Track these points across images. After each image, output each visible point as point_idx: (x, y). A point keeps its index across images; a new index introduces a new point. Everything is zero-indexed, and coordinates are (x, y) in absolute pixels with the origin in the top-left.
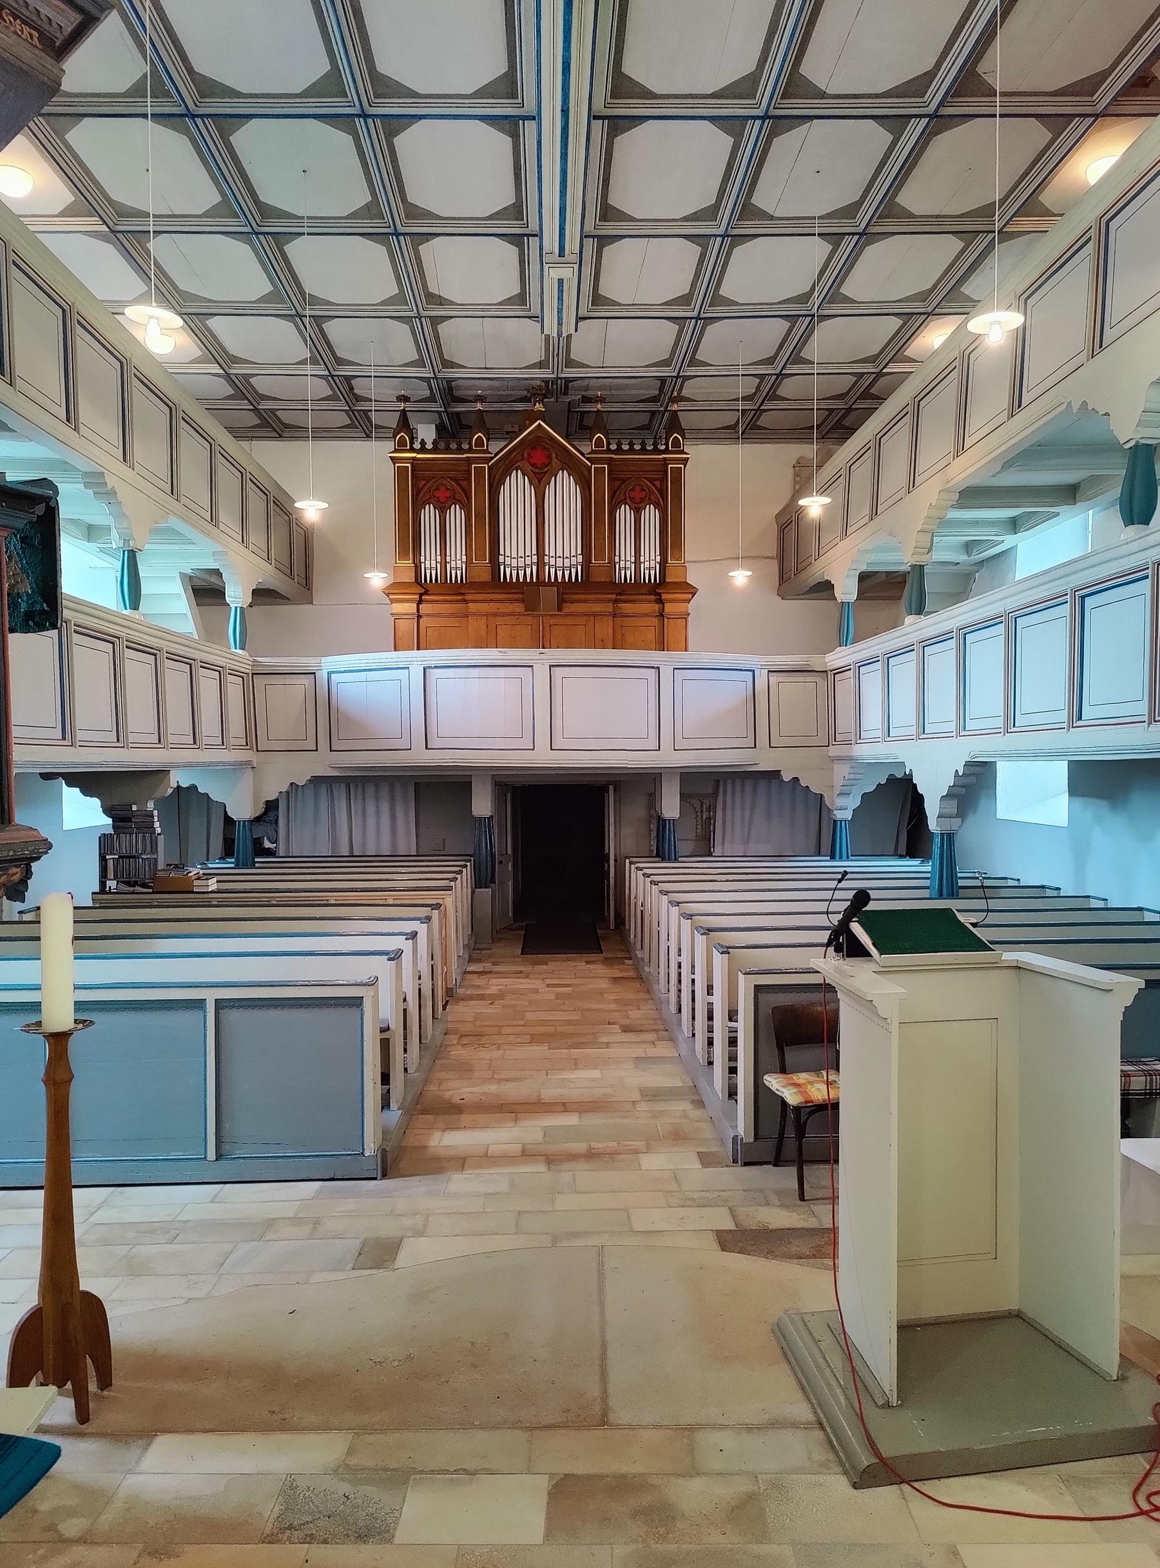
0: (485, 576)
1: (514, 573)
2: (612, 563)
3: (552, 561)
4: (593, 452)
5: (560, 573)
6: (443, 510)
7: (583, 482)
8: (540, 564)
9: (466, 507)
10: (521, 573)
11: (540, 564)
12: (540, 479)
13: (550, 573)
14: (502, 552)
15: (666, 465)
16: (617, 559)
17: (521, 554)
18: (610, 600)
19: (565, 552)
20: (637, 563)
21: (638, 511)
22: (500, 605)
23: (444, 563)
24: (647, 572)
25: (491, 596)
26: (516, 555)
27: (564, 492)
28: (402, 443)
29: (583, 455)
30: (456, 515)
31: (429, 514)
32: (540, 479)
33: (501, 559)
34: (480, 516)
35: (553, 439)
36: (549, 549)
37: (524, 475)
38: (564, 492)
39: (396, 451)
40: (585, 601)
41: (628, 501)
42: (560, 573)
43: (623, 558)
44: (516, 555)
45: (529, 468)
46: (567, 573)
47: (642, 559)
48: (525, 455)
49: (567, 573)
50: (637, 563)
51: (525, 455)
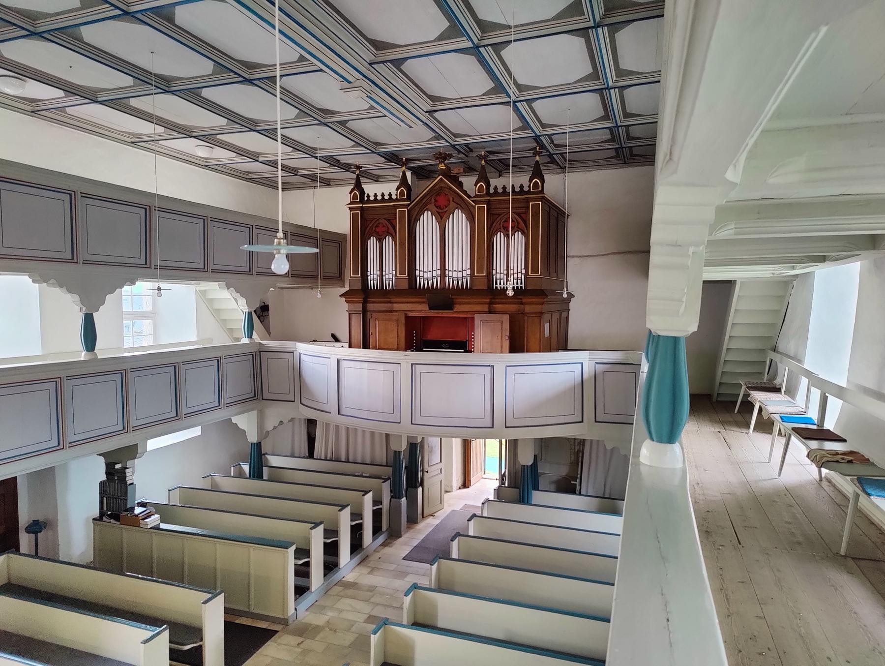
0: (405, 286)
1: (426, 282)
2: (490, 276)
3: (451, 274)
4: (476, 196)
6: (380, 241)
7: (471, 218)
8: (443, 275)
10: (430, 282)
11: (443, 275)
12: (442, 217)
13: (449, 282)
14: (418, 268)
15: (528, 203)
16: (494, 272)
18: (485, 303)
19: (459, 267)
22: (414, 305)
23: (382, 276)
25: (406, 300)
26: (427, 270)
27: (459, 224)
28: (355, 197)
29: (469, 197)
30: (388, 243)
31: (372, 243)
32: (442, 217)
34: (402, 244)
35: (450, 188)
36: (449, 265)
37: (433, 214)
38: (459, 224)
40: (469, 303)
41: (502, 230)
42: (455, 282)
44: (427, 270)
45: (435, 209)
46: (455, 282)
47: (511, 272)
49: (460, 282)
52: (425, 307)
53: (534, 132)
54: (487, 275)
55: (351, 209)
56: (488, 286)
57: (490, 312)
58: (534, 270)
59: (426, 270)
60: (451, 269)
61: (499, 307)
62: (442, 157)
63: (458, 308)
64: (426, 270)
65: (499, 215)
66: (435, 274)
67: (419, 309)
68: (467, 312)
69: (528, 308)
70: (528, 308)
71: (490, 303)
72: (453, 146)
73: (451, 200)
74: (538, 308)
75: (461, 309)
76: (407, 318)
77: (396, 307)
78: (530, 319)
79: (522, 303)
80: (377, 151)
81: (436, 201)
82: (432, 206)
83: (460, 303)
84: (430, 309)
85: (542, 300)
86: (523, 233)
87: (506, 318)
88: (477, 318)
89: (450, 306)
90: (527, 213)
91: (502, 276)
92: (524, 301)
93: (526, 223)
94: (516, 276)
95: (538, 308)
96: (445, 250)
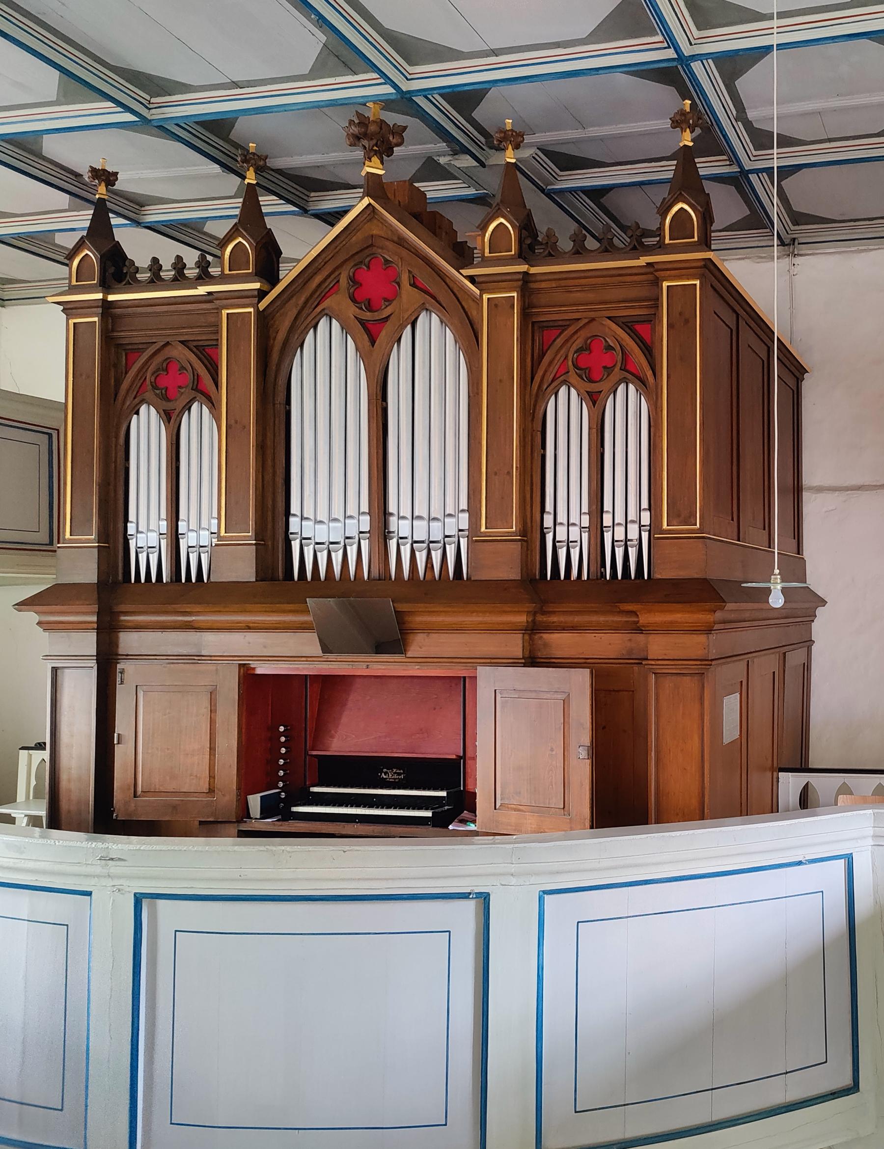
5: (421, 558)
6: (172, 419)
7: (469, 336)
9: (214, 407)
10: (337, 558)
12: (375, 335)
13: (401, 556)
15: (656, 283)
16: (548, 521)
17: (338, 513)
18: (513, 628)
20: (597, 530)
21: (595, 400)
23: (175, 537)
24: (620, 552)
32: (375, 335)
33: (294, 523)
38: (432, 362)
39: (72, 290)
41: (573, 377)
42: (421, 558)
43: (562, 517)
45: (351, 310)
47: (607, 520)
48: (344, 281)
50: (597, 530)
51: (344, 281)
52: (306, 644)
53: (672, 43)
54: (524, 532)
55: (69, 309)
56: (525, 563)
57: (532, 660)
58: (681, 512)
59: (322, 515)
60: (406, 511)
61: (560, 642)
62: (375, 137)
63: (421, 645)
64: (322, 515)
65: (563, 327)
66: (353, 532)
67: (287, 649)
68: (452, 660)
69: (658, 646)
70: (658, 646)
71: (532, 629)
72: (404, 102)
73: (405, 279)
74: (694, 645)
75: (433, 648)
76: (253, 686)
77: (212, 642)
78: (668, 684)
79: (638, 629)
80: (155, 115)
81: (354, 280)
82: (340, 301)
83: (429, 629)
84: (326, 649)
85: (709, 618)
86: (642, 383)
87: (581, 679)
88: (489, 681)
89: (392, 643)
90: (652, 319)
91: (575, 533)
92: (644, 619)
93: (649, 351)
94: (620, 534)
95: (694, 645)
96: (391, 451)
